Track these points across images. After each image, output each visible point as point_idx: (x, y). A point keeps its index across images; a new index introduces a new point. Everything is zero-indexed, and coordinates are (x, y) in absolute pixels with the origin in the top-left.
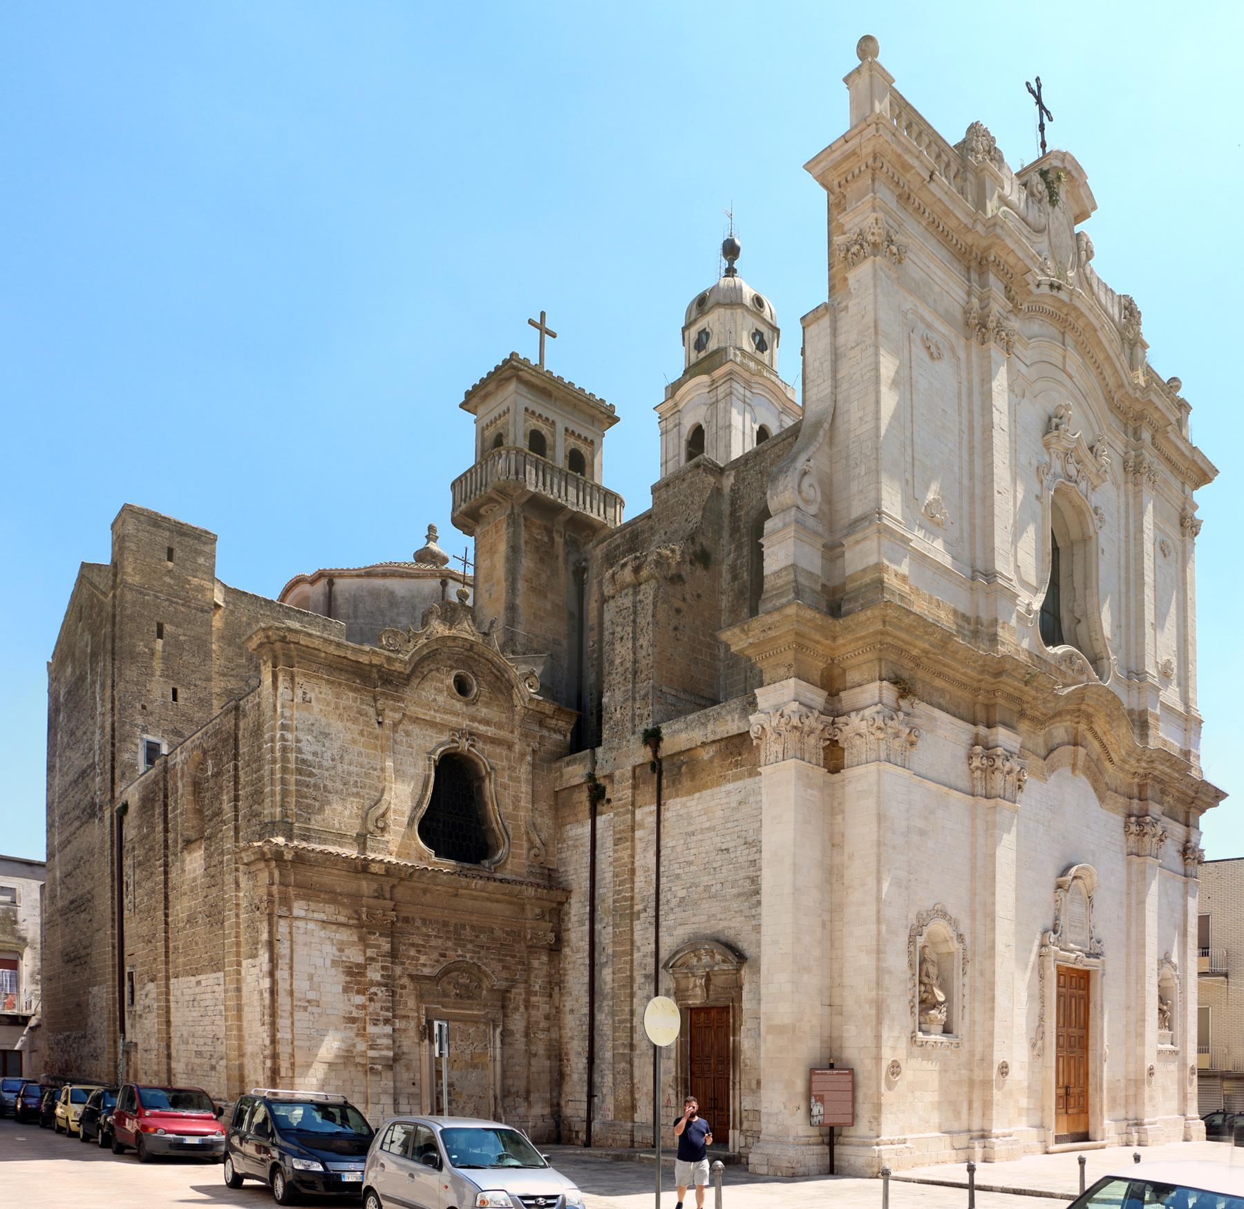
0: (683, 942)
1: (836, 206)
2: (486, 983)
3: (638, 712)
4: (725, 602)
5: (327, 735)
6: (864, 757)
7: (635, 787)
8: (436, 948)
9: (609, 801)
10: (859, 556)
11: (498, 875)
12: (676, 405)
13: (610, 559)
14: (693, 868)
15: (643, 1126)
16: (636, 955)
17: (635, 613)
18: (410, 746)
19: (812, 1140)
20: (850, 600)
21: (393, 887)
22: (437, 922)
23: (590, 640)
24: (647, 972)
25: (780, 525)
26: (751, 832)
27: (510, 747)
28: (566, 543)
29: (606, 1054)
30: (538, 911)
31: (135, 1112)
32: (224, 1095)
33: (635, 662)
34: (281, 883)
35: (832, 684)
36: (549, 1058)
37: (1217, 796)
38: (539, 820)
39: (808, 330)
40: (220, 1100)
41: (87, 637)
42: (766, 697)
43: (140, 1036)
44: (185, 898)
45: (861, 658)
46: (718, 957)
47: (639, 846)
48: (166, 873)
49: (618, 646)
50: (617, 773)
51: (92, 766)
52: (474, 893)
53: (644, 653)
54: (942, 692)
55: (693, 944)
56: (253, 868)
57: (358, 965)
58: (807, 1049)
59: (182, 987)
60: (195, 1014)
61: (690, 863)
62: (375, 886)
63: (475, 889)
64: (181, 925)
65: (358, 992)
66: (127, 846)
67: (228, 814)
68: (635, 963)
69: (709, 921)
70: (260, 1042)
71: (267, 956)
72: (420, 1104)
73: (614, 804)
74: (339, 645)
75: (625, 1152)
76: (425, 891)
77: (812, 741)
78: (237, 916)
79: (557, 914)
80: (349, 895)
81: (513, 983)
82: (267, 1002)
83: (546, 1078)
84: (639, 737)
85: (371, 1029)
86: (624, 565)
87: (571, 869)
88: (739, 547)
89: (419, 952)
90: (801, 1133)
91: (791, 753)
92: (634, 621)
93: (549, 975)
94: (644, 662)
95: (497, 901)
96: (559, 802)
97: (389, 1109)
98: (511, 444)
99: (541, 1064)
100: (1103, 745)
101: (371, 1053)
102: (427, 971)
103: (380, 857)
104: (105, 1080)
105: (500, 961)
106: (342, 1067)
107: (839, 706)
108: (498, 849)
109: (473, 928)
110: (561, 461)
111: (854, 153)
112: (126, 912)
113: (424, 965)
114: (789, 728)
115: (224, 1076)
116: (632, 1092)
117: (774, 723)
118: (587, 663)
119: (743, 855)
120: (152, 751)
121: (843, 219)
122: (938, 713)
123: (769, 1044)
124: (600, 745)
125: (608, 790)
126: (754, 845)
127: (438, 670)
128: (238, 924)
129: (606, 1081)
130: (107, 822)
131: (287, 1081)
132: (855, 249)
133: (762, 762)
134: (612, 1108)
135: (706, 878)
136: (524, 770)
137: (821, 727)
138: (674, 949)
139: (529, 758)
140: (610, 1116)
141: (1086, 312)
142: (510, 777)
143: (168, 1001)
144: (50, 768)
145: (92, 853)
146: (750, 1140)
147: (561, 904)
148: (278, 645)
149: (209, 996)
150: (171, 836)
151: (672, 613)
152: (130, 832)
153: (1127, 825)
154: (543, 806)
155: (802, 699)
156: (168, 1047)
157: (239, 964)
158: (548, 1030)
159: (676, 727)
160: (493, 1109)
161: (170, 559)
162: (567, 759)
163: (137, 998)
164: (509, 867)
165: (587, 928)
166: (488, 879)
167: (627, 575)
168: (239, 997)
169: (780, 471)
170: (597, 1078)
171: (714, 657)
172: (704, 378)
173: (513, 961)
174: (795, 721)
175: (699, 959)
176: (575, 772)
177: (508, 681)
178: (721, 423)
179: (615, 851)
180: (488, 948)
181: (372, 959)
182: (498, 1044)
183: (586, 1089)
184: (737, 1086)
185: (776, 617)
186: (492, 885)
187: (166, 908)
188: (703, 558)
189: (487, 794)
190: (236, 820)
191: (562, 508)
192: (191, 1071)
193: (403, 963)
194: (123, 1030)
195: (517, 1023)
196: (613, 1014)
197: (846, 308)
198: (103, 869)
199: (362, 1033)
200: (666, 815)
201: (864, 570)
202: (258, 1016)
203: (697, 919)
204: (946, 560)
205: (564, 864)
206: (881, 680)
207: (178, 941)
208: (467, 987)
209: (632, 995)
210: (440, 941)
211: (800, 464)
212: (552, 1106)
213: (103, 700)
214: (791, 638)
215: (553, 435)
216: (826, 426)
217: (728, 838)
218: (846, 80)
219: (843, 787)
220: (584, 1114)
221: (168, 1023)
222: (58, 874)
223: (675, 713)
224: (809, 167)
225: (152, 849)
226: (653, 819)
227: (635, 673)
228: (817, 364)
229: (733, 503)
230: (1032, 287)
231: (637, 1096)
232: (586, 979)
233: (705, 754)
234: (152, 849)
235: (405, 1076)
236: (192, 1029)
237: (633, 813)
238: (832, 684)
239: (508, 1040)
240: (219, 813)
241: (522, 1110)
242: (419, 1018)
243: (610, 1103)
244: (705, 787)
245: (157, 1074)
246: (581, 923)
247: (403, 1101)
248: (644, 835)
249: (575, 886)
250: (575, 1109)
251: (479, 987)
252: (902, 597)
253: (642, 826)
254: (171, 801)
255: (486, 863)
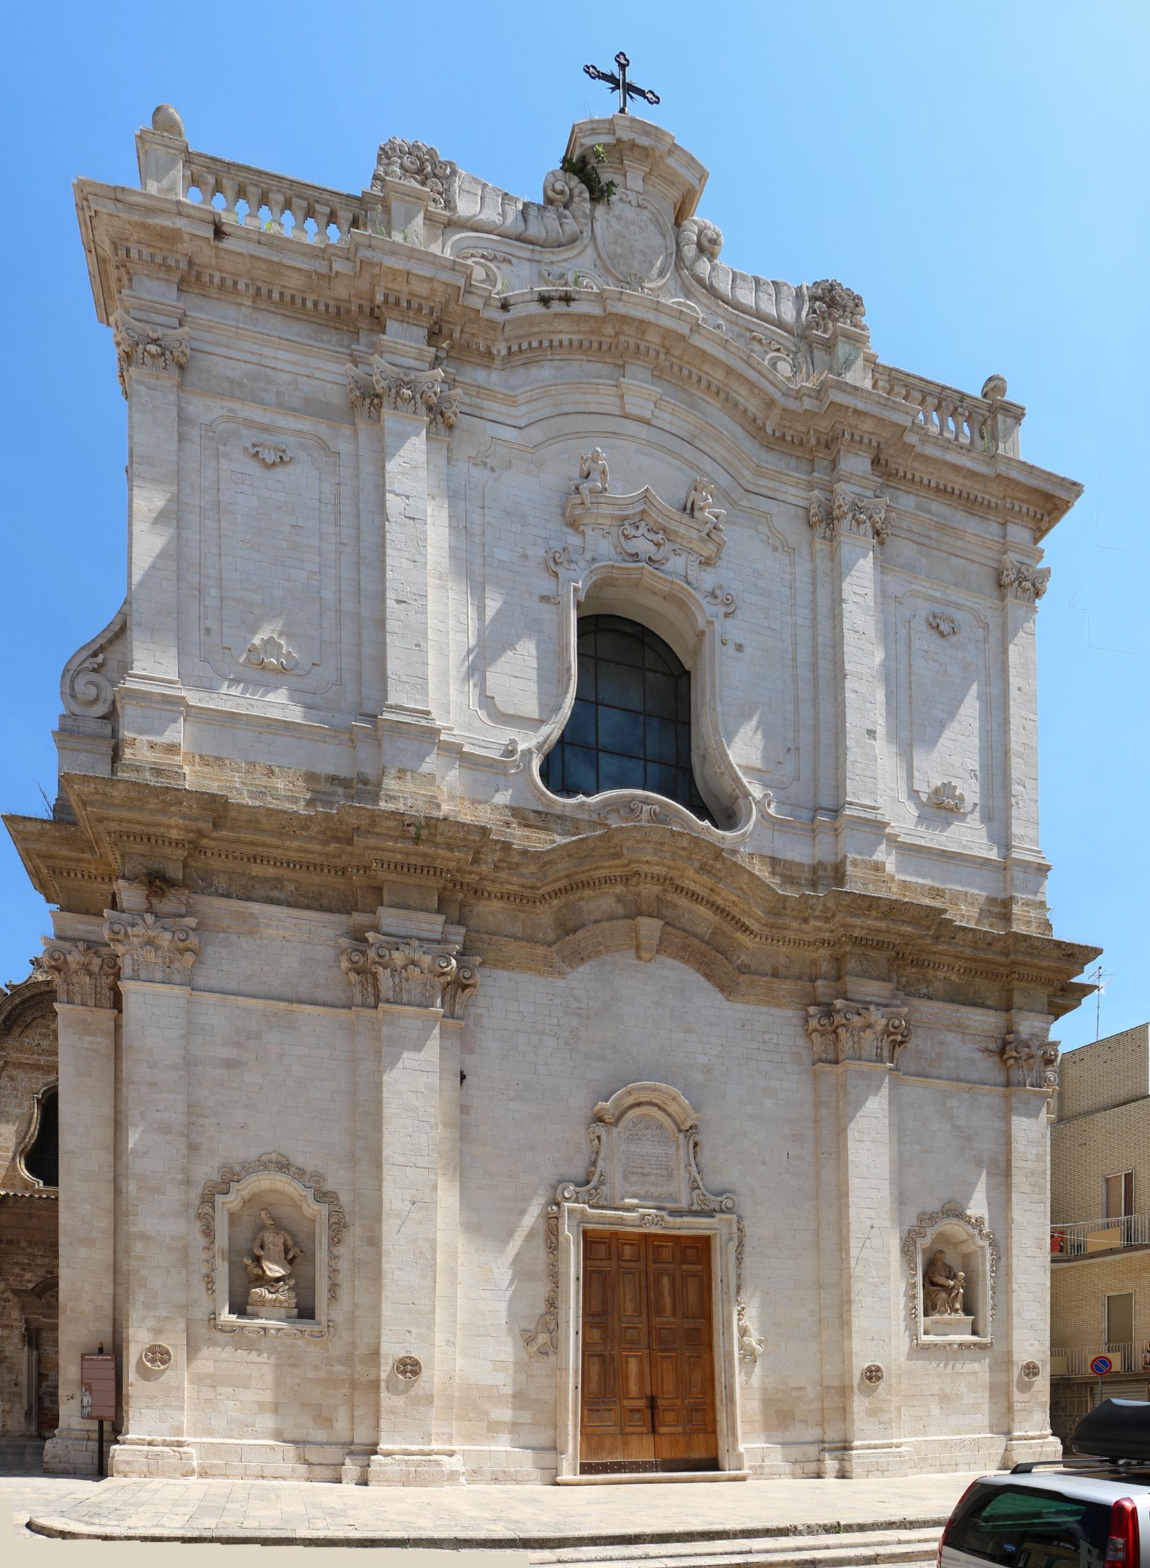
18: (15, 1089)
113: (30, 1281)
127: (43, 1017)
210: (47, 1260)
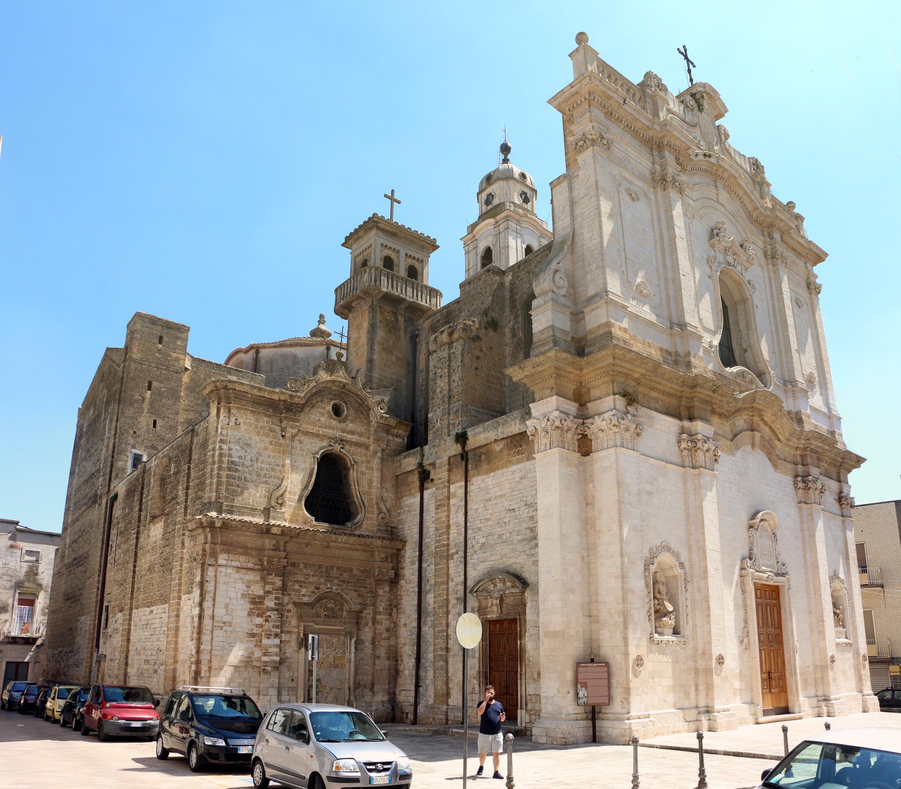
0: (484, 574)
1: (568, 122)
2: (346, 607)
3: (452, 422)
4: (508, 351)
5: (248, 445)
6: (605, 444)
7: (450, 470)
8: (313, 583)
9: (432, 480)
10: (594, 319)
11: (357, 532)
12: (474, 236)
13: (433, 329)
14: (490, 523)
15: (455, 708)
16: (451, 584)
17: (450, 360)
19: (579, 716)
20: (590, 346)
21: (286, 542)
22: (314, 565)
23: (421, 378)
24: (458, 596)
25: (542, 302)
26: (530, 498)
27: (367, 447)
28: (405, 320)
29: (429, 655)
30: (383, 555)
31: (100, 704)
32: (161, 691)
33: (450, 390)
34: (212, 543)
35: (581, 398)
36: (388, 659)
37: (859, 461)
38: (385, 495)
39: (555, 190)
40: (158, 694)
41: (105, 391)
42: (536, 409)
43: (108, 650)
44: (148, 555)
45: (600, 381)
46: (509, 584)
47: (453, 509)
48: (137, 538)
49: (438, 381)
50: (438, 462)
51: (98, 471)
52: (340, 545)
53: (455, 385)
54: (657, 399)
55: (491, 575)
56: (194, 533)
57: (259, 597)
58: (574, 648)
59: (140, 615)
60: (146, 634)
61: (488, 520)
62: (274, 542)
63: (341, 542)
64: (144, 572)
65: (258, 616)
66: (114, 521)
67: (182, 498)
68: (450, 590)
69: (501, 558)
70: (189, 652)
71: (198, 592)
72: (296, 695)
73: (435, 482)
74: (260, 389)
75: (441, 728)
76: (307, 545)
77: (569, 435)
78: (181, 565)
79: (396, 557)
80: (256, 549)
81: (364, 606)
82: (196, 624)
83: (385, 673)
84: (453, 437)
85: (265, 641)
86: (443, 331)
87: (406, 527)
88: (516, 317)
89: (301, 586)
90: (571, 712)
91: (555, 444)
92: (449, 366)
93: (390, 600)
94: (456, 390)
95: (356, 550)
96: (399, 483)
97: (275, 699)
98: (372, 264)
99: (383, 663)
100: (770, 428)
101: (264, 659)
102: (305, 599)
103: (278, 523)
104: (82, 682)
105: (356, 591)
106: (243, 669)
107: (586, 412)
108: (358, 514)
109: (338, 568)
110: (403, 272)
111: (577, 93)
112: (108, 565)
113: (304, 595)
114: (553, 428)
115: (162, 677)
116: (447, 683)
117: (543, 425)
118: (418, 393)
119: (524, 513)
120: (137, 459)
121: (573, 128)
122: (654, 414)
123: (546, 645)
124: (426, 443)
125: (432, 473)
126: (532, 506)
127: (322, 401)
128: (181, 571)
129: (428, 675)
130: (104, 506)
131: (205, 680)
132: (581, 143)
133: (536, 448)
134: (432, 695)
135: (499, 530)
136: (376, 463)
137: (575, 426)
138: (478, 579)
139: (379, 454)
140: (431, 701)
141: (729, 168)
142: (367, 468)
143: (130, 625)
144: (72, 473)
145: (91, 526)
146: (533, 717)
147: (399, 550)
148: (222, 391)
149: (157, 621)
150: (143, 513)
151: (474, 359)
152: (117, 513)
153: (795, 483)
154: (388, 485)
155: (561, 409)
156: (127, 657)
157: (179, 598)
158: (388, 639)
159: (477, 430)
160: (347, 698)
161: (160, 343)
162: (404, 454)
163: (109, 623)
164: (364, 526)
165: (416, 566)
166: (350, 535)
167: (445, 337)
168: (178, 621)
169: (541, 271)
170: (422, 673)
171: (502, 385)
172: (491, 221)
173: (365, 591)
174: (557, 423)
175: (495, 586)
176: (410, 462)
177: (367, 406)
178: (502, 245)
179: (436, 513)
180: (348, 582)
181: (269, 592)
182: (353, 650)
183: (414, 681)
184: (523, 677)
185: (542, 358)
186: (352, 539)
187: (135, 561)
188: (493, 325)
189: (351, 479)
190: (186, 502)
191: (403, 300)
192: (140, 674)
193: (290, 595)
194: (98, 646)
195: (367, 634)
196: (434, 626)
197: (578, 175)
198: (97, 537)
199: (259, 645)
200: (471, 488)
201: (599, 327)
202: (189, 634)
203: (493, 558)
204: (653, 318)
205: (402, 523)
206: (614, 394)
207: (141, 584)
208: (333, 609)
209: (448, 613)
210: (316, 578)
211: (553, 265)
212: (389, 694)
213: (110, 429)
214: (552, 370)
215: (398, 258)
216: (569, 243)
217: (514, 502)
218: (570, 55)
219: (592, 465)
220: (412, 700)
221: (128, 640)
222: (68, 541)
223: (477, 421)
224: (550, 102)
225: (130, 523)
226: (462, 491)
227: (450, 397)
228: (561, 208)
229: (511, 291)
230: (693, 157)
231: (450, 686)
232: (416, 602)
233: (497, 447)
234: (130, 523)
235: (287, 674)
236: (144, 644)
237: (449, 488)
238: (581, 398)
239: (360, 647)
240: (175, 498)
241: (368, 698)
242: (299, 633)
243: (431, 692)
244: (497, 468)
245: (117, 676)
246: (413, 563)
247: (284, 693)
248: (456, 502)
249: (409, 538)
250: (406, 696)
251: (341, 610)
252: (625, 342)
253: (454, 496)
254: (145, 491)
255: (349, 524)
